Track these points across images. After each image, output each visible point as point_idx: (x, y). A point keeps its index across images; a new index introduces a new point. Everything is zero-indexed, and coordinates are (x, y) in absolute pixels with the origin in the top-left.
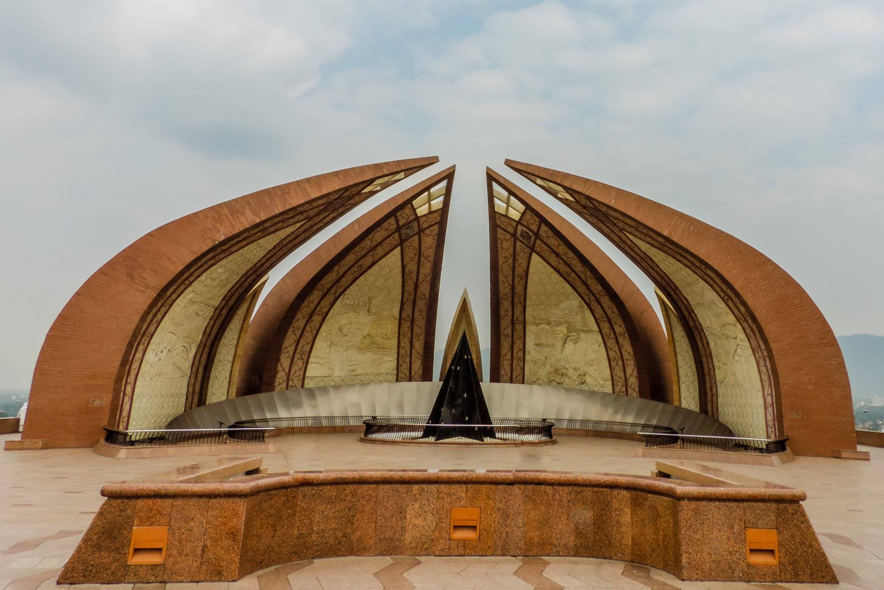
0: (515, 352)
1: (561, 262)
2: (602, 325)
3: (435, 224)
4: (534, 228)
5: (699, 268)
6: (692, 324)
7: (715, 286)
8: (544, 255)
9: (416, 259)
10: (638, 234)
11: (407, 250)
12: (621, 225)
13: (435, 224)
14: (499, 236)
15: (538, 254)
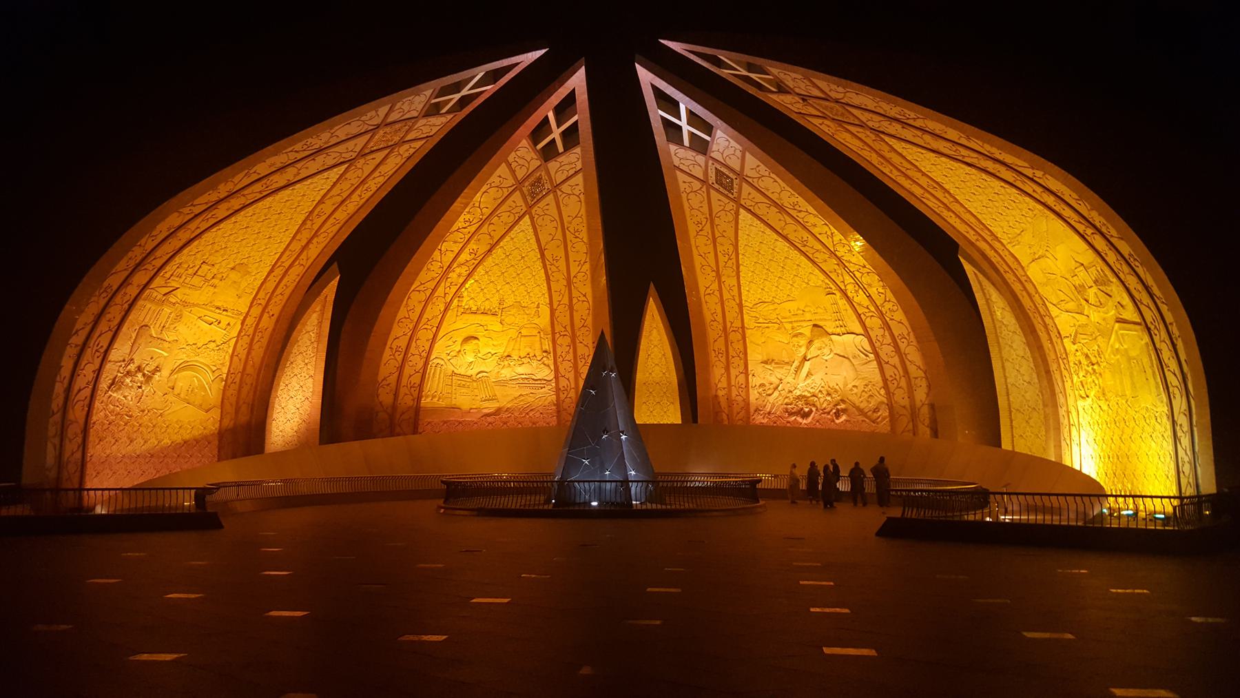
0: (733, 377)
1: (789, 220)
2: (868, 322)
3: (576, 173)
4: (735, 164)
5: (1032, 179)
6: (1026, 302)
7: (1067, 213)
8: (758, 213)
9: (559, 235)
10: (908, 134)
11: (539, 222)
12: (875, 122)
13: (576, 173)
14: (682, 186)
15: (749, 211)
